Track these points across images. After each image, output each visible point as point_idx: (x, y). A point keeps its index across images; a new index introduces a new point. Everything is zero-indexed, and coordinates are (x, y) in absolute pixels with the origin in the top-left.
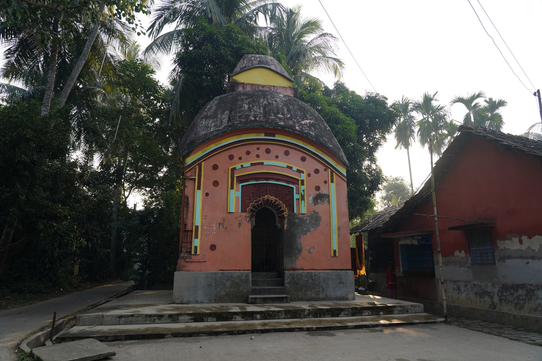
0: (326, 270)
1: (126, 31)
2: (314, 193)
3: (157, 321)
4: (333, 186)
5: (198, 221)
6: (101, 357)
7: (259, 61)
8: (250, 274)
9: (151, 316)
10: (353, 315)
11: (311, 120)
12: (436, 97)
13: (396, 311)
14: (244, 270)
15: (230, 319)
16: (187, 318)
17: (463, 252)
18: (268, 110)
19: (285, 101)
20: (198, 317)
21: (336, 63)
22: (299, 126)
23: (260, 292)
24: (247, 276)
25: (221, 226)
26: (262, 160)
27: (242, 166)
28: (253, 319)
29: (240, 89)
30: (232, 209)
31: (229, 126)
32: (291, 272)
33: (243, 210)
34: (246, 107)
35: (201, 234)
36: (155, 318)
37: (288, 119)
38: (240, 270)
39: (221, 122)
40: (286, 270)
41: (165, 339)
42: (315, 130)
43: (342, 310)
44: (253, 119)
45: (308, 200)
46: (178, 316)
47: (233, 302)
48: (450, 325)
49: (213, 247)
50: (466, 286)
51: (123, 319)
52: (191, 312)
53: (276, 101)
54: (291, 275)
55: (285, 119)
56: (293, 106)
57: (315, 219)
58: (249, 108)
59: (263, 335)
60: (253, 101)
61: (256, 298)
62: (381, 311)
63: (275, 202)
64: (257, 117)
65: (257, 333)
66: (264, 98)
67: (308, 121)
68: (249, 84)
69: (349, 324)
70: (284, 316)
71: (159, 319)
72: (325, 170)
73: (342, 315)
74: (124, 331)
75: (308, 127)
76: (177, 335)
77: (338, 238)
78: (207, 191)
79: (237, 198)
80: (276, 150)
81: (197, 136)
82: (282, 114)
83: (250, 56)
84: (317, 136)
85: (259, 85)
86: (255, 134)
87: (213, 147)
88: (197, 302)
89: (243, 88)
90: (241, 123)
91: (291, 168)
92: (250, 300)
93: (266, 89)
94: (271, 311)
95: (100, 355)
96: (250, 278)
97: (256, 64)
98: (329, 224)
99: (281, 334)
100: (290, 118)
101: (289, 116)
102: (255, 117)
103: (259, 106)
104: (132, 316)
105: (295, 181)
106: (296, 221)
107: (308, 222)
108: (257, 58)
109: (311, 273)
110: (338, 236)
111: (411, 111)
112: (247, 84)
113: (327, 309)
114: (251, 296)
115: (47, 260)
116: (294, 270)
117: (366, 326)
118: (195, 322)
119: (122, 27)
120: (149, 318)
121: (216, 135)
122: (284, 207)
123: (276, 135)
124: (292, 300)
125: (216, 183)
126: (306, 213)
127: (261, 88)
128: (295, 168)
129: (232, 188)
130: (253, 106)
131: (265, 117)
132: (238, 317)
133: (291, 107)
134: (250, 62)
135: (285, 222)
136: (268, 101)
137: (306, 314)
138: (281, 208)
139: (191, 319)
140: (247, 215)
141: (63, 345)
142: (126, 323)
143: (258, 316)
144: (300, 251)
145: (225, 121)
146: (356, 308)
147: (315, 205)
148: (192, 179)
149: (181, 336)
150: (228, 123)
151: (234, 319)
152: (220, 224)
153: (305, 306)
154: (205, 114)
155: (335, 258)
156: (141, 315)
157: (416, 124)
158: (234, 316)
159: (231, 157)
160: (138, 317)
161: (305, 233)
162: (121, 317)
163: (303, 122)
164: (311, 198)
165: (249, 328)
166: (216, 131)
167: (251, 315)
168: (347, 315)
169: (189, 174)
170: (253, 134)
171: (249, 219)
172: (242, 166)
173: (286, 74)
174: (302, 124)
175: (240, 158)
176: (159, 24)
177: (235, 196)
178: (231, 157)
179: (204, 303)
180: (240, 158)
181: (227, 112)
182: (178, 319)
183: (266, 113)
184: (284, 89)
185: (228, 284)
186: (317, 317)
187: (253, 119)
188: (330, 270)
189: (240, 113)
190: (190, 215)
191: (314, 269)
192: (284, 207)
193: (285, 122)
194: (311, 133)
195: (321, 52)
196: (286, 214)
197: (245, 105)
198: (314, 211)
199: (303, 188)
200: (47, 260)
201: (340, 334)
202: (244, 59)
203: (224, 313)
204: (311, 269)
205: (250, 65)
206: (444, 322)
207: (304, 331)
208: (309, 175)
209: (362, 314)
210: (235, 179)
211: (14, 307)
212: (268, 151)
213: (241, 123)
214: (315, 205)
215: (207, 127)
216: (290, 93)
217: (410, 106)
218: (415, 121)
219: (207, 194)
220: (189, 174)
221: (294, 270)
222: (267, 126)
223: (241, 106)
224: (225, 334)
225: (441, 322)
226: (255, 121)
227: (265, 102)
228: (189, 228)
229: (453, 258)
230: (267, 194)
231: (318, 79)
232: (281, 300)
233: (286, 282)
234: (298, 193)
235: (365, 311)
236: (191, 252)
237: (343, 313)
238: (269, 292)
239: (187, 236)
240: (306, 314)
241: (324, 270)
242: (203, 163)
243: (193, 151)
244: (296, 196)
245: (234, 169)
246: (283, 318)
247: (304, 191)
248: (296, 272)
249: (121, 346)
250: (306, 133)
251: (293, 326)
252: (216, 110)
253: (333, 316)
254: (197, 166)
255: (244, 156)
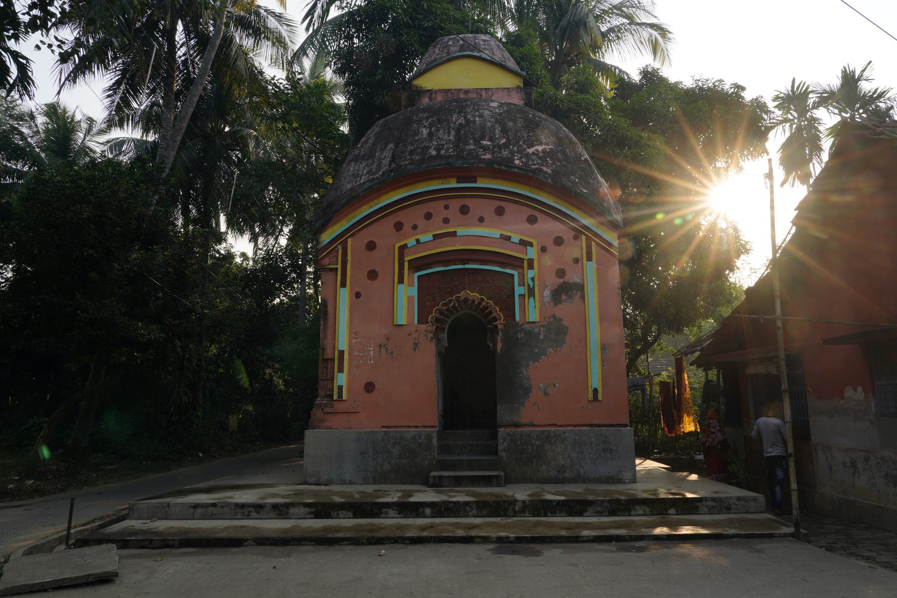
0: (579, 426)
1: (285, 27)
2: (553, 281)
3: (254, 514)
4: (590, 268)
5: (343, 342)
6: (90, 579)
7: (462, 46)
8: (435, 435)
9: (243, 506)
10: (612, 513)
11: (547, 144)
12: (866, 74)
13: (705, 509)
14: (425, 427)
15: (377, 515)
16: (303, 510)
17: (859, 389)
18: (462, 135)
19: (500, 114)
20: (322, 510)
21: (655, 33)
22: (520, 159)
23: (452, 466)
24: (429, 437)
25: (383, 350)
26: (453, 227)
27: (418, 241)
28: (418, 516)
29: (425, 101)
30: (402, 317)
31: (391, 171)
32: (510, 430)
33: (422, 320)
34: (425, 132)
35: (350, 365)
36: (251, 509)
37: (500, 147)
38: (417, 427)
39: (380, 164)
40: (501, 426)
41: (242, 549)
42: (554, 163)
43: (590, 503)
44: (434, 153)
45: (542, 296)
46: (288, 508)
47: (405, 483)
48: (809, 542)
49: (370, 387)
50: (867, 460)
51: (199, 510)
52: (310, 501)
53: (481, 116)
54: (509, 435)
55: (494, 147)
56: (515, 122)
57: (557, 331)
58: (430, 134)
59: (411, 547)
60: (439, 121)
61: (441, 477)
62: (671, 507)
63: (480, 303)
64: (442, 149)
65: (403, 543)
66: (459, 113)
67: (540, 148)
68: (440, 91)
69: (586, 533)
70: (475, 511)
71: (258, 512)
72: (576, 238)
73: (589, 514)
74: (187, 531)
75: (540, 158)
76: (265, 541)
77: (603, 365)
78: (358, 290)
79: (410, 299)
80: (478, 207)
81: (338, 193)
82: (490, 140)
83: (446, 38)
84: (556, 174)
85: (459, 90)
86: (440, 181)
87: (365, 211)
88: (343, 482)
89: (430, 99)
90: (412, 162)
91: (508, 238)
92: (431, 480)
93: (471, 95)
94: (451, 502)
95: (89, 575)
96: (435, 441)
97: (456, 52)
98: (584, 340)
99: (445, 548)
100: (505, 146)
101: (503, 141)
102: (438, 149)
103: (449, 128)
104: (214, 505)
105: (516, 263)
106: (519, 336)
107: (542, 337)
108: (458, 41)
109: (549, 431)
110: (603, 361)
111: (813, 108)
112: (437, 92)
113: (559, 501)
114: (432, 474)
115: (172, 408)
116: (516, 425)
117: (618, 539)
118: (316, 517)
119: (279, 21)
120: (258, 509)
121: (368, 189)
122: (497, 312)
123: (479, 179)
124: (508, 481)
125: (373, 275)
126: (537, 320)
127: (462, 96)
128: (516, 238)
129: (401, 281)
130: (438, 130)
131: (456, 147)
132: (391, 512)
133: (511, 124)
134: (446, 50)
135: (499, 338)
136: (465, 117)
137: (517, 508)
138: (491, 313)
139: (311, 513)
140: (430, 328)
141: (86, 550)
142: (204, 517)
143: (428, 511)
144: (527, 391)
145: (386, 162)
146: (618, 501)
147: (555, 305)
148: (331, 270)
149: (271, 545)
150: (390, 165)
151: (383, 515)
152: (381, 345)
153: (521, 494)
154: (356, 152)
155: (595, 404)
156: (225, 505)
157: (826, 133)
158: (384, 510)
159: (399, 226)
160: (223, 507)
161: (536, 357)
162: (196, 506)
163: (531, 151)
164: (547, 293)
165: (399, 534)
166: (370, 181)
167: (415, 509)
168: (600, 514)
169: (326, 261)
170: (436, 181)
171: (431, 335)
172: (418, 241)
173: (512, 64)
174: (527, 155)
175: (415, 227)
176: (322, 6)
177: (406, 295)
178: (399, 226)
179: (354, 483)
180: (415, 227)
181: (391, 145)
182: (287, 513)
183: (460, 140)
184: (505, 93)
185: (396, 451)
186: (539, 515)
187: (434, 153)
188: (587, 425)
189: (412, 144)
190: (329, 333)
191: (555, 425)
192: (497, 312)
193: (493, 153)
194: (545, 169)
195: (627, 17)
196: (500, 323)
197: (424, 130)
198: (554, 316)
199: (530, 274)
200: (172, 408)
201: (554, 553)
202: (434, 47)
203: (367, 503)
204: (550, 425)
205: (444, 55)
206: (795, 536)
207: (491, 542)
208: (544, 249)
209: (630, 511)
210: (406, 264)
211: (106, 483)
212: (464, 210)
213: (412, 162)
214: (555, 305)
215: (356, 176)
216: (517, 100)
217: (812, 98)
218: (821, 128)
219: (358, 295)
220: (326, 261)
221: (516, 425)
222: (459, 163)
223: (417, 133)
224: (345, 542)
225: (785, 535)
226: (438, 156)
227: (461, 120)
228: (328, 354)
229: (842, 402)
230: (464, 289)
231: (616, 68)
232: (487, 481)
233: (500, 448)
234: (522, 284)
235: (637, 507)
236: (332, 396)
237: (591, 510)
238: (470, 466)
239: (327, 368)
240: (517, 508)
241: (575, 426)
242: (349, 240)
243: (330, 219)
244: (519, 290)
245: (403, 248)
246: (474, 516)
247: (533, 279)
248: (520, 430)
249: (159, 559)
250: (534, 171)
251: (474, 533)
252: (374, 144)
253: (571, 514)
254: (340, 247)
255: (421, 223)
